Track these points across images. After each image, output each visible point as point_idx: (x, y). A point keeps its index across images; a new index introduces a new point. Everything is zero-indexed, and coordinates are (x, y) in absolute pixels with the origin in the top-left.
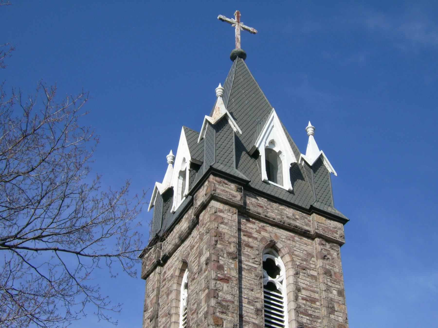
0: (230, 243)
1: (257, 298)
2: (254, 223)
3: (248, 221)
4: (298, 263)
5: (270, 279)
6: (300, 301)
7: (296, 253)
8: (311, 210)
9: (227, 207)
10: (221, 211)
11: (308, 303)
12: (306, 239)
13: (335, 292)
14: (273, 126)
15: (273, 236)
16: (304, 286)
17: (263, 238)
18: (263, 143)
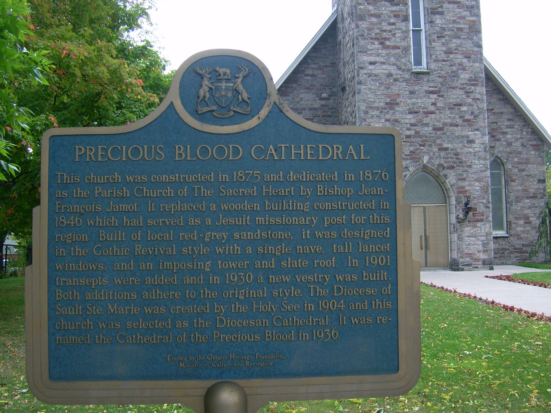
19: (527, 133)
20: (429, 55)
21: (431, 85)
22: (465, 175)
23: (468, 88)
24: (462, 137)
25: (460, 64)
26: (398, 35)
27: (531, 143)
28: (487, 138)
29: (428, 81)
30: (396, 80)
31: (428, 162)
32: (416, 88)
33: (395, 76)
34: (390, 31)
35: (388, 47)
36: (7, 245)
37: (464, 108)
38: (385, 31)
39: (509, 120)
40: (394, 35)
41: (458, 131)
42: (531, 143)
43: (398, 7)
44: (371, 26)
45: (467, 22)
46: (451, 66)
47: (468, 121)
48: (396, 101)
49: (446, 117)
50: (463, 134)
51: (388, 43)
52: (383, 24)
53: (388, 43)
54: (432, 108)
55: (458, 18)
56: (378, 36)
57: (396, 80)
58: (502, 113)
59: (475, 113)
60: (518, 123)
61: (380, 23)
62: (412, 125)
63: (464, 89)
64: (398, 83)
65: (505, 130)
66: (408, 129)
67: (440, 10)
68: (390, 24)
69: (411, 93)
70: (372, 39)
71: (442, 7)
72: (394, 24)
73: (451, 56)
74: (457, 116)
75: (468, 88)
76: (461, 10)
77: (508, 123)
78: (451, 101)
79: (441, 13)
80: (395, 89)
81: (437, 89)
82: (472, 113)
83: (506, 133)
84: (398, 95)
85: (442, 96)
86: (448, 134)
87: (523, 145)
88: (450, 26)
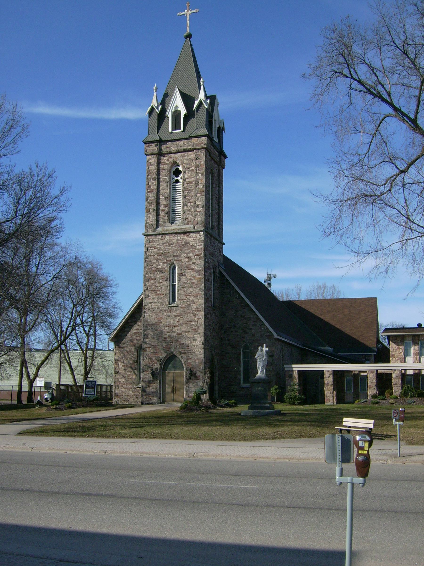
0: (153, 173)
1: (166, 192)
2: (167, 156)
3: (164, 156)
4: (185, 167)
5: (176, 178)
6: (185, 185)
7: (185, 162)
8: (191, 138)
9: (153, 156)
10: (150, 160)
11: (189, 185)
12: (191, 152)
13: (200, 175)
14: (176, 97)
15: (174, 159)
16: (187, 177)
17: (171, 162)
18: (171, 111)
19: (264, 328)
20: (178, 298)
21: (178, 312)
22: (191, 357)
23: (195, 313)
24: (191, 337)
25: (193, 301)
26: (163, 288)
27: (266, 334)
28: (203, 338)
29: (176, 310)
30: (161, 310)
31: (174, 351)
32: (171, 314)
33: (161, 309)
34: (160, 286)
35: (158, 295)
36: (35, 386)
37: (193, 323)
38: (157, 286)
39: (254, 322)
40: (161, 288)
41: (190, 335)
42: (266, 334)
43: (164, 274)
44: (151, 284)
45: (197, 279)
46: (188, 302)
47: (195, 329)
48: (160, 321)
49: (184, 328)
50: (192, 336)
51: (158, 292)
52: (157, 283)
53: (158, 292)
54: (177, 324)
55: (193, 277)
56: (154, 289)
57: (161, 310)
58: (250, 318)
59: (198, 325)
60: (259, 323)
61: (156, 283)
62: (168, 332)
63: (193, 313)
64: (161, 312)
65: (251, 327)
66: (165, 335)
67: (184, 273)
68: (160, 283)
69: (168, 316)
70: (152, 291)
71: (184, 272)
72: (162, 283)
73: (188, 297)
74: (189, 328)
75: (195, 313)
76: (194, 273)
77: (254, 323)
78: (186, 320)
79: (185, 275)
80: (160, 315)
81: (180, 314)
82: (197, 325)
83: (252, 329)
84: (161, 318)
85: (182, 318)
86: (185, 336)
87: (261, 335)
88: (188, 281)
